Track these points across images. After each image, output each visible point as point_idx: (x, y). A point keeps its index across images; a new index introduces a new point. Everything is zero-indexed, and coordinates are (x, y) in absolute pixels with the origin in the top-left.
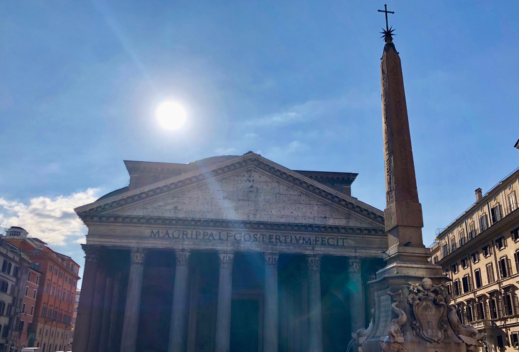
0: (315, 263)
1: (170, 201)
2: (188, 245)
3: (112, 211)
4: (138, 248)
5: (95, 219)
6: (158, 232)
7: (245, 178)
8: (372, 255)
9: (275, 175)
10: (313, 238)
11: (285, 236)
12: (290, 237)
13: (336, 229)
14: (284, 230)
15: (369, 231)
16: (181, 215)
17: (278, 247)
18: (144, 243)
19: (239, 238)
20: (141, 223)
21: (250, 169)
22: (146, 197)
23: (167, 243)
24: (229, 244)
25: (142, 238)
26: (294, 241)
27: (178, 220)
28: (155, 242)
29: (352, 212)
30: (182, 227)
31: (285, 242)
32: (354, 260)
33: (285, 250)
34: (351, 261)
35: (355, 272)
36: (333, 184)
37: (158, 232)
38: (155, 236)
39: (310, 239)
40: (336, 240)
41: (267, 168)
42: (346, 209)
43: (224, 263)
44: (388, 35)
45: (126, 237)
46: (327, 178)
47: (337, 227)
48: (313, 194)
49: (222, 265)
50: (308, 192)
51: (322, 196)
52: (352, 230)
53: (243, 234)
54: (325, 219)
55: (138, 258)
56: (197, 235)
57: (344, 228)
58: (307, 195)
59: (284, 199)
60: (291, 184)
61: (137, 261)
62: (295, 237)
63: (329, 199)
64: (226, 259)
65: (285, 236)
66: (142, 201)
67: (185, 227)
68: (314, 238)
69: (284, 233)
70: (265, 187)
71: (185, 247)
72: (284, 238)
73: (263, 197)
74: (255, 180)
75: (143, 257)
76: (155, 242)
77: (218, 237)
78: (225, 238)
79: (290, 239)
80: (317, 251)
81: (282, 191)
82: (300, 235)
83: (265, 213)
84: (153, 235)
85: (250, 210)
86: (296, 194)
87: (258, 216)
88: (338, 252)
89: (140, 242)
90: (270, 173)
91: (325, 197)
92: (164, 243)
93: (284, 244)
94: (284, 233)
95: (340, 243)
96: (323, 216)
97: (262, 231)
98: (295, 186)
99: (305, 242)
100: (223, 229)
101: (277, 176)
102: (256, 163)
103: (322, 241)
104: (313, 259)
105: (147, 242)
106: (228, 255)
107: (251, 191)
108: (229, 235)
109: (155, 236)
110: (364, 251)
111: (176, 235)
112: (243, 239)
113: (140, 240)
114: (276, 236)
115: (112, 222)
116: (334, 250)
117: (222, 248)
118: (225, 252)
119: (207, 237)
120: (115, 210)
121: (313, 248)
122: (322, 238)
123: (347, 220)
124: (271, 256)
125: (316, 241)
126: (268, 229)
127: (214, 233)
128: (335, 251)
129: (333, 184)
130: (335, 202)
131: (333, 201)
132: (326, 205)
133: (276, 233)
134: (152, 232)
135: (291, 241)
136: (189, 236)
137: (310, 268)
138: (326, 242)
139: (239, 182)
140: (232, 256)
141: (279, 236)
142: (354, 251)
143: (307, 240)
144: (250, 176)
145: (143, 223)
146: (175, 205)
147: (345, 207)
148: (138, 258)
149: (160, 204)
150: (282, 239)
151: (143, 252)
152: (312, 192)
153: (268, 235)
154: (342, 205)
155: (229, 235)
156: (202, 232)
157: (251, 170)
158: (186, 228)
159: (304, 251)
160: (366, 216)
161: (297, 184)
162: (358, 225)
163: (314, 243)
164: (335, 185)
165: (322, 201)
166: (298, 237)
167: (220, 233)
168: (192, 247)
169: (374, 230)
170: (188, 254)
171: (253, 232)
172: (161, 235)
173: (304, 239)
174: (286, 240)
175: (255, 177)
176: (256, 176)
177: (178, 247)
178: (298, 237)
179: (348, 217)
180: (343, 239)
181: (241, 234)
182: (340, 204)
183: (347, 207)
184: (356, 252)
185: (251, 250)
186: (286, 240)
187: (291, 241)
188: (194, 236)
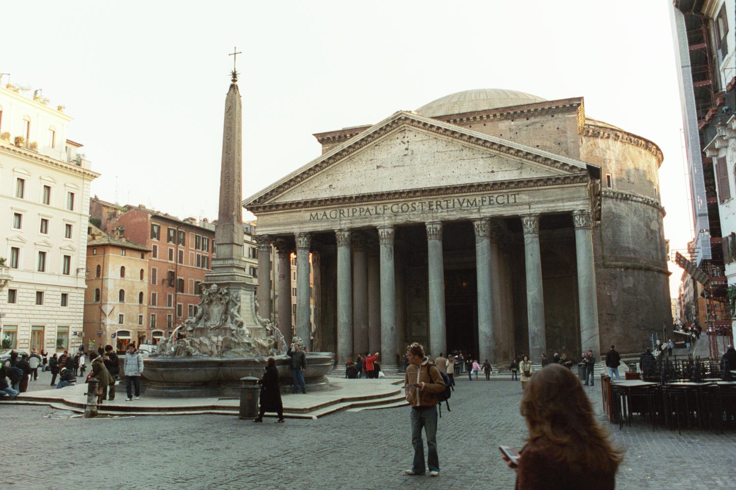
0: (481, 227)
1: (325, 180)
2: (345, 224)
3: (273, 199)
4: (300, 233)
5: (260, 210)
6: (317, 214)
7: (399, 141)
8: (550, 209)
9: (431, 131)
10: (479, 199)
11: (447, 201)
12: (452, 201)
13: (502, 185)
14: (444, 194)
15: (546, 181)
16: (336, 194)
17: (439, 214)
18: (306, 227)
19: (397, 210)
20: (299, 208)
21: (403, 129)
22: (302, 181)
23: (326, 224)
24: (386, 218)
25: (302, 223)
26: (457, 205)
27: (333, 200)
28: (314, 225)
29: (524, 160)
30: (337, 206)
31: (447, 208)
32: (528, 218)
33: (447, 217)
34: (524, 220)
35: (528, 232)
36: (553, 116)
37: (317, 214)
38: (314, 218)
39: (475, 200)
40: (506, 197)
41: (421, 125)
42: (517, 158)
43: (382, 239)
44: (234, 75)
45: (289, 224)
46: (543, 109)
47: (502, 183)
48: (477, 146)
49: (381, 241)
50: (470, 144)
51: (487, 147)
52: (528, 183)
53: (400, 205)
54: (493, 174)
55: (301, 243)
56: (353, 213)
57: (511, 182)
58: (470, 148)
59: (444, 158)
60: (450, 138)
61: (301, 246)
62: (458, 200)
63: (495, 149)
64: (385, 233)
65: (447, 201)
66: (299, 184)
67: (340, 205)
68: (480, 199)
69: (445, 198)
70: (422, 147)
71: (343, 226)
72: (446, 202)
73: (419, 160)
74: (410, 141)
75: (306, 242)
76: (314, 225)
77: (374, 212)
78: (381, 212)
79: (452, 203)
80: (484, 213)
81: (441, 149)
82: (463, 198)
83: (423, 177)
84: (312, 218)
85: (407, 177)
86: (457, 149)
87: (415, 181)
88: (508, 211)
89: (301, 226)
90: (425, 129)
91: (490, 148)
92: (323, 224)
93: (445, 210)
94: (445, 198)
95: (511, 200)
96: (490, 171)
97: (419, 198)
98: (455, 140)
99: (469, 205)
100: (378, 202)
101: (433, 131)
102: (408, 122)
103: (490, 200)
104: (479, 222)
105: (307, 225)
106: (386, 230)
107: (405, 155)
108: (386, 208)
109: (314, 218)
110: (540, 206)
111: (333, 215)
112: (400, 210)
113: (300, 224)
114: (437, 202)
115: (275, 211)
116: (504, 209)
117: (379, 223)
118: (384, 227)
119: (363, 214)
120: (276, 197)
121: (479, 210)
122: (490, 197)
123: (519, 171)
124: (431, 226)
125: (483, 201)
126: (426, 196)
127: (370, 207)
128: (505, 211)
129: (553, 116)
130: (502, 152)
131: (500, 151)
132: (492, 156)
133: (436, 198)
134: (311, 215)
135: (454, 205)
136: (346, 215)
137: (477, 233)
138: (495, 201)
139: (393, 146)
140: (390, 231)
141: (440, 202)
142: (528, 207)
143: (472, 202)
144: (404, 137)
145: (302, 207)
146: (330, 184)
147: (514, 155)
148: (301, 243)
149: (317, 184)
150: (444, 204)
151: (305, 236)
152: (474, 143)
153: (427, 203)
154: (511, 154)
155: (386, 208)
156: (358, 208)
157: (404, 130)
158: (342, 207)
159: (467, 216)
160: (541, 163)
161: (456, 138)
162: (534, 175)
163: (481, 204)
164: (556, 116)
165: (489, 152)
166: (461, 199)
167: (376, 207)
168: (349, 226)
169: (549, 179)
170: (346, 234)
171: (411, 201)
172: (320, 217)
173: (468, 201)
174: (447, 205)
175: (409, 138)
176: (410, 136)
177: (336, 227)
178: (461, 199)
179: (521, 167)
180: (515, 195)
181: (398, 204)
182: (508, 153)
183: (517, 156)
184: (530, 208)
185: (409, 221)
186: (447, 205)
187: (454, 205)
188: (351, 214)
